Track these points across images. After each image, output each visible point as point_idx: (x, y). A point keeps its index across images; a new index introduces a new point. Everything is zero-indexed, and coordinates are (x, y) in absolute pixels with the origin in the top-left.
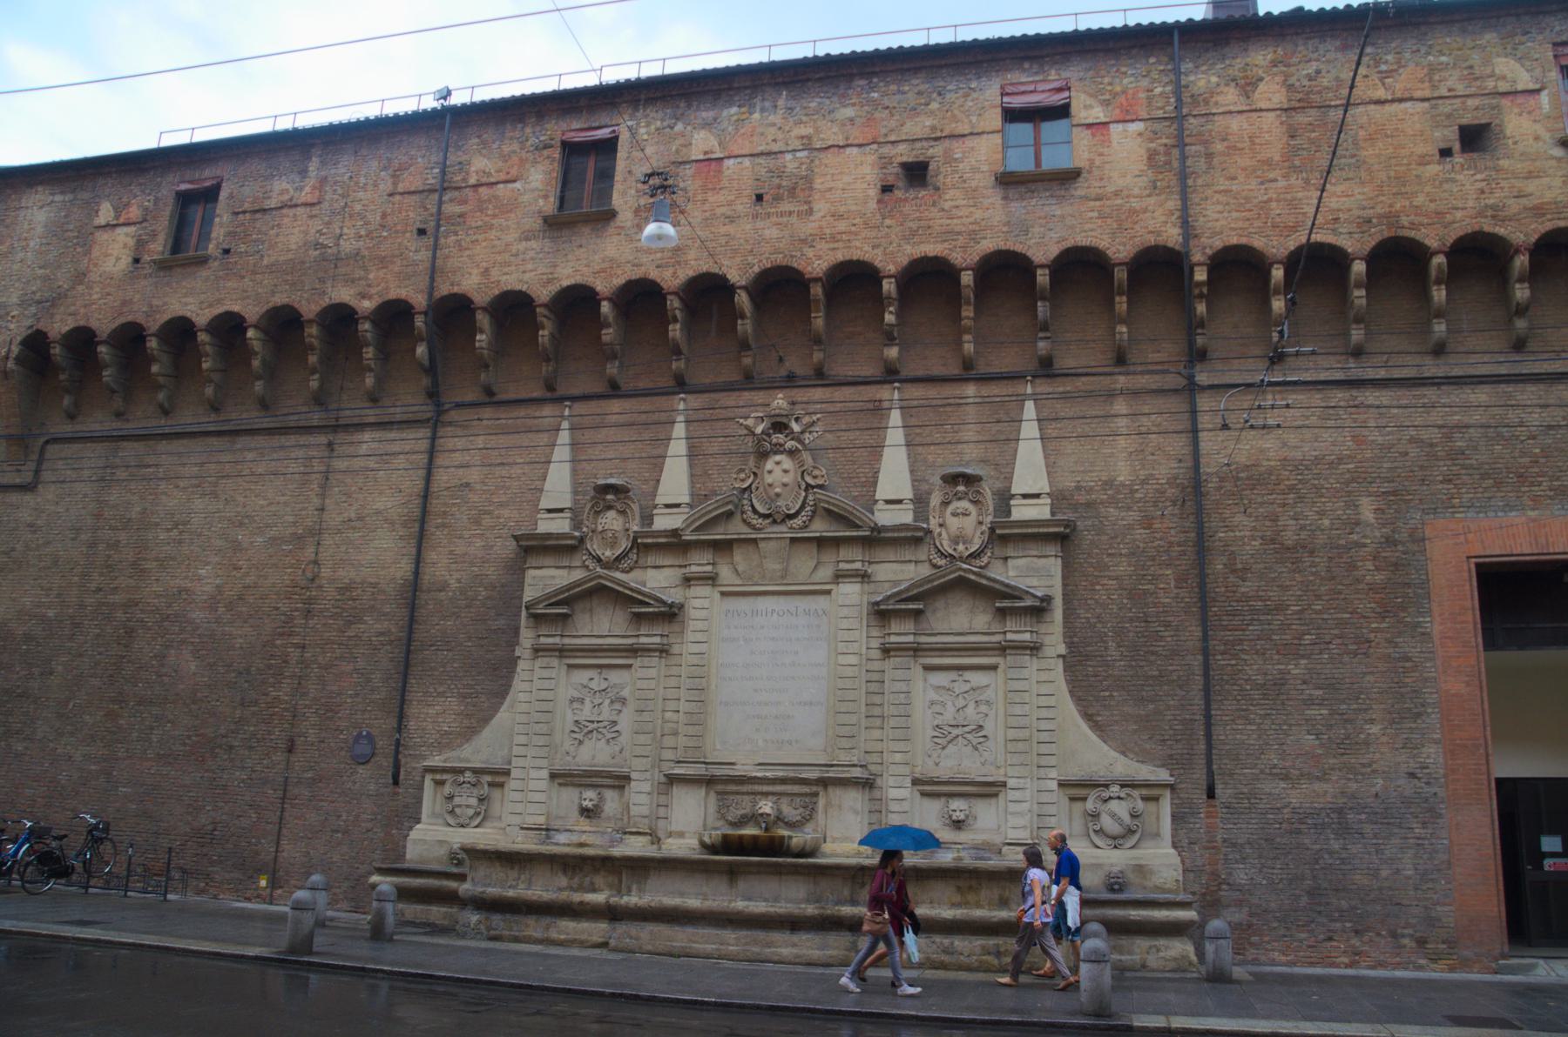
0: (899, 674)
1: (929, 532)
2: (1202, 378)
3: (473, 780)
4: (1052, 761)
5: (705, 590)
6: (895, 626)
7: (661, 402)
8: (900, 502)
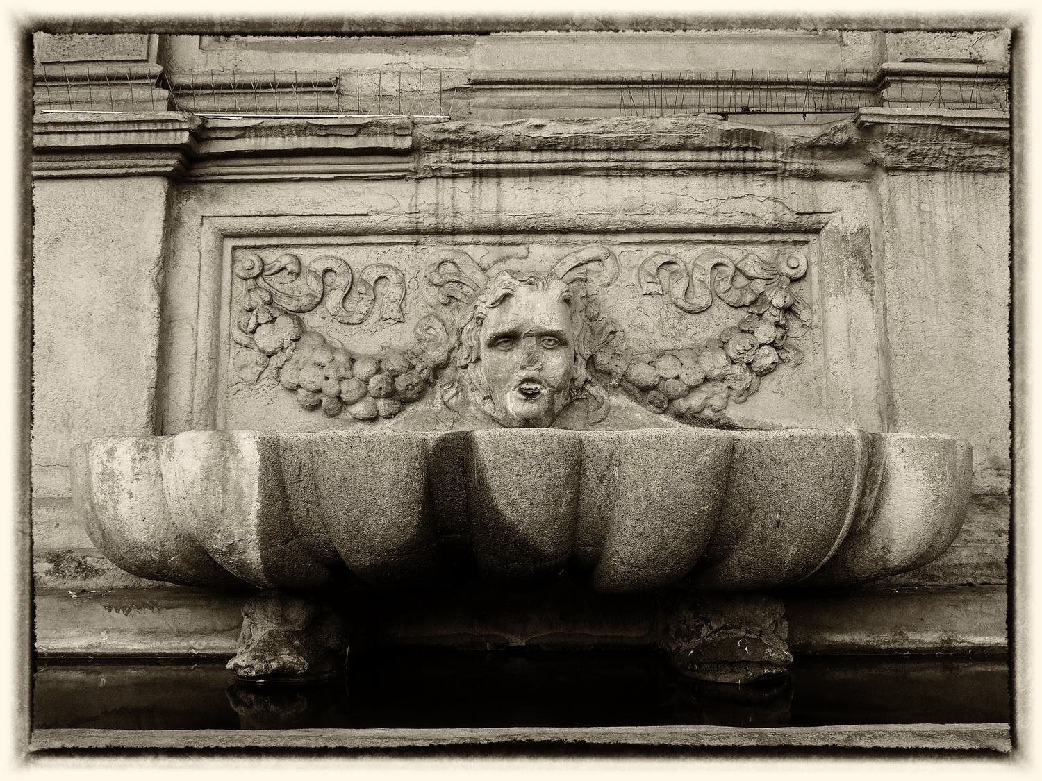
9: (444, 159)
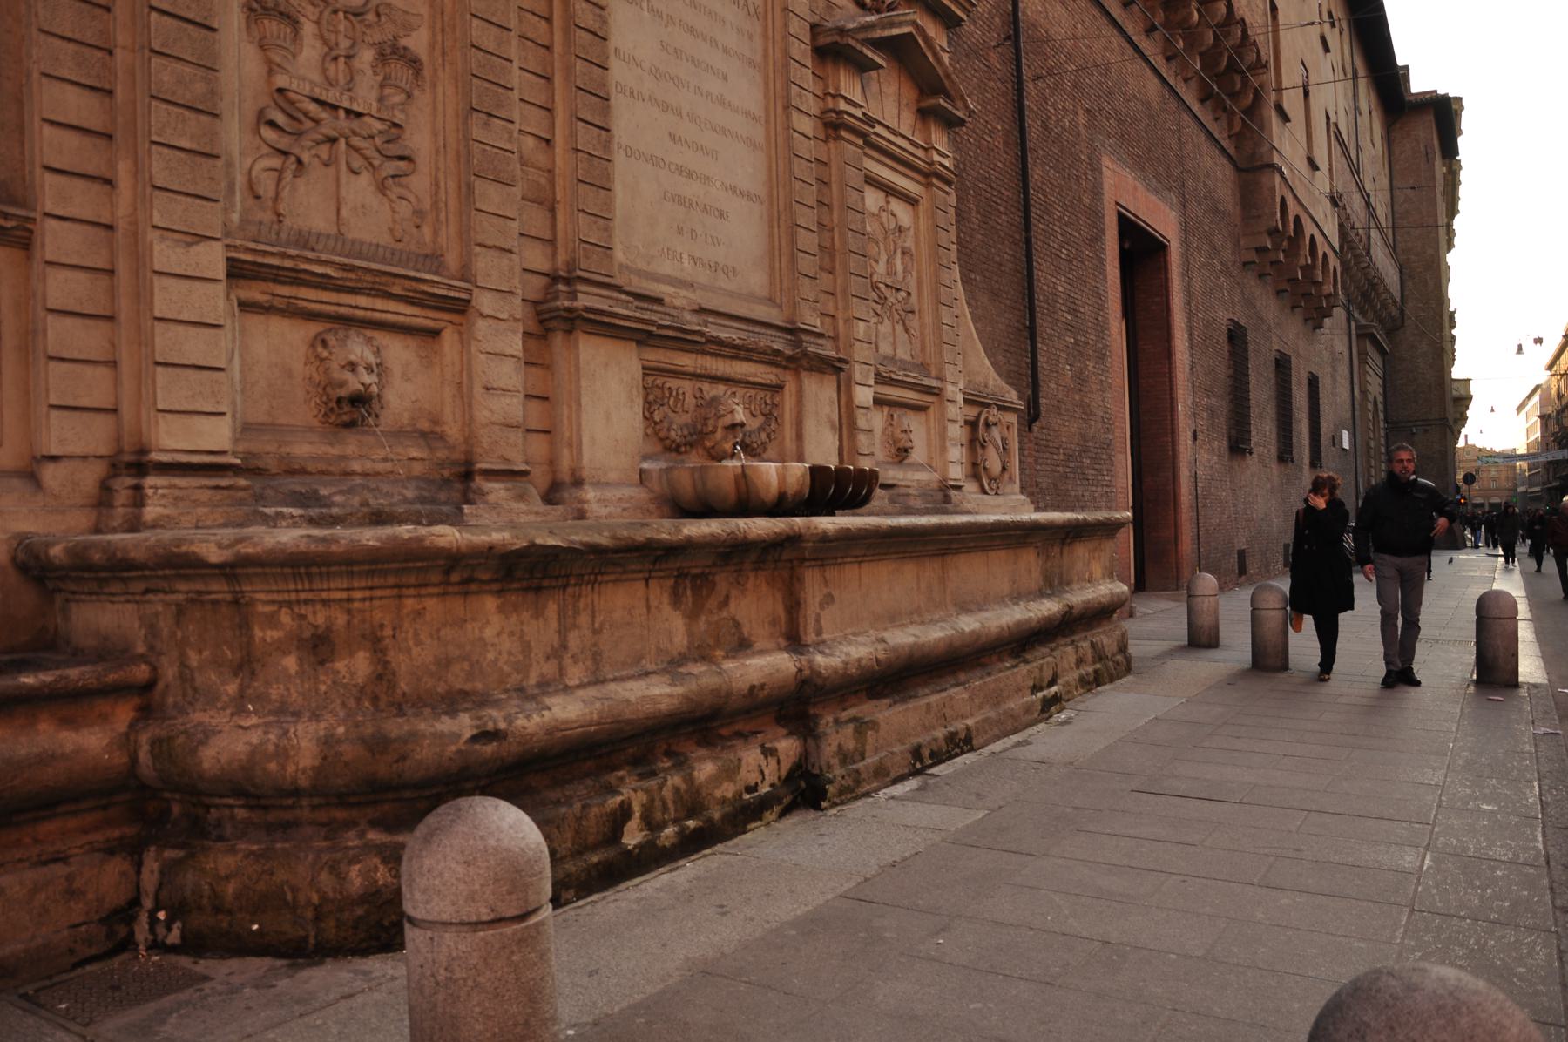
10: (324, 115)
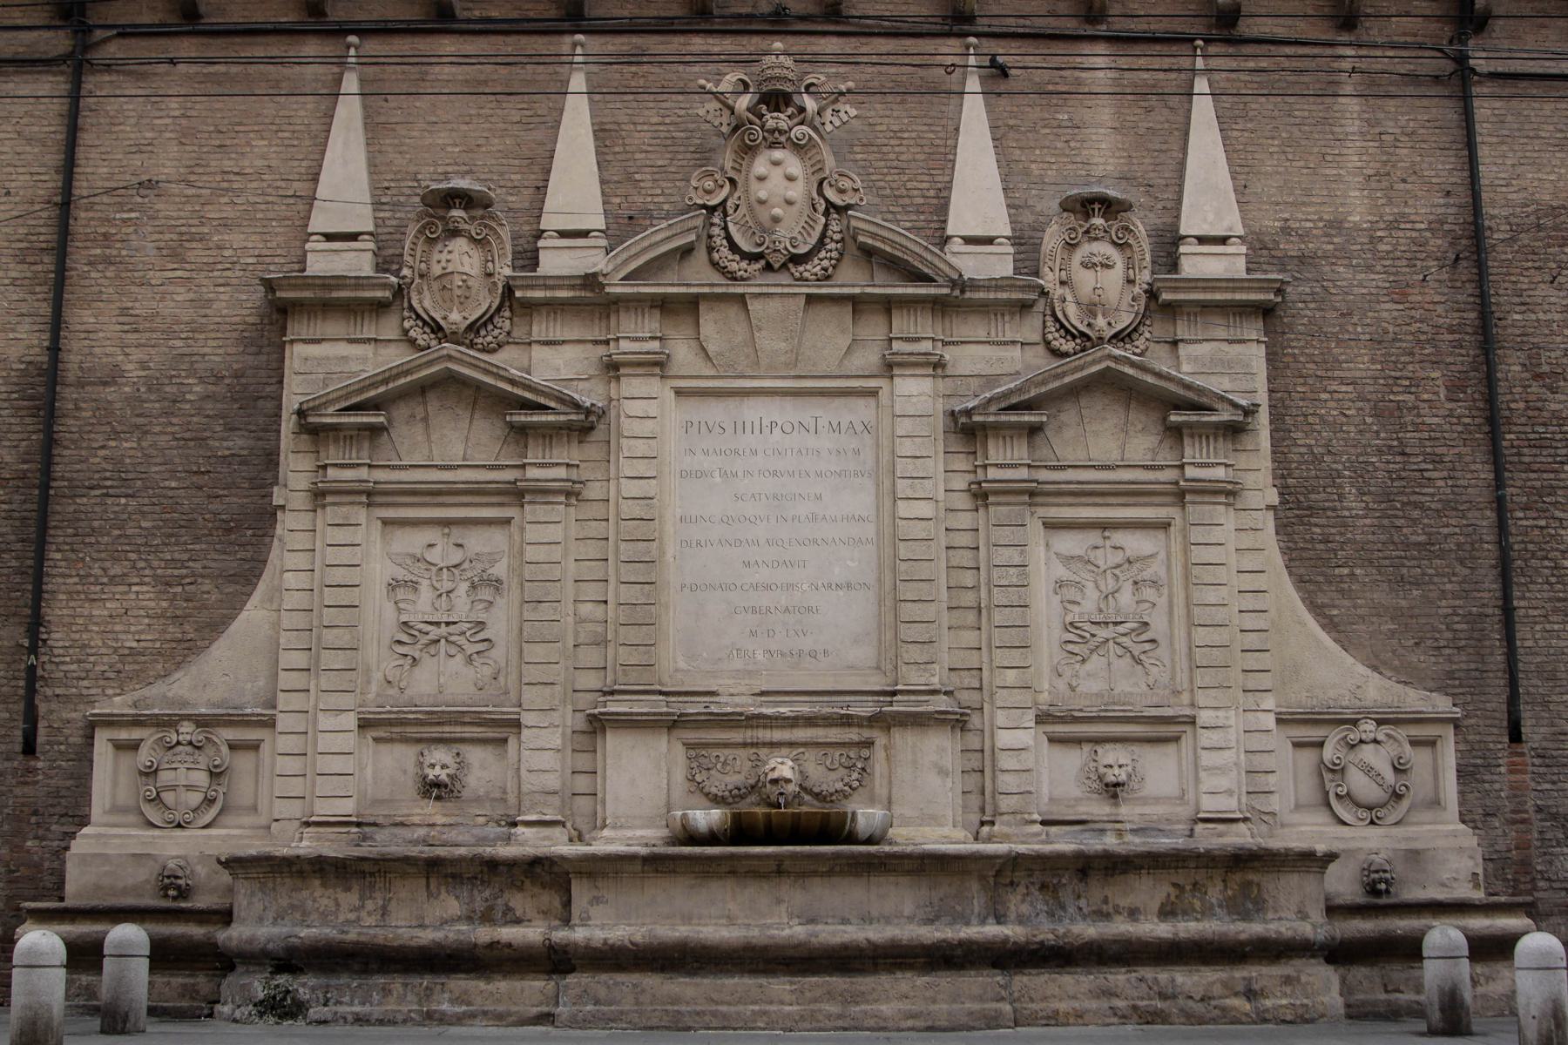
0: (1004, 535)
1: (1044, 293)
2: (1480, 63)
3: (198, 737)
4: (1265, 681)
5: (653, 386)
6: (996, 452)
7: (538, 44)
8: (989, 241)
9: (754, 722)
10: (430, 628)
